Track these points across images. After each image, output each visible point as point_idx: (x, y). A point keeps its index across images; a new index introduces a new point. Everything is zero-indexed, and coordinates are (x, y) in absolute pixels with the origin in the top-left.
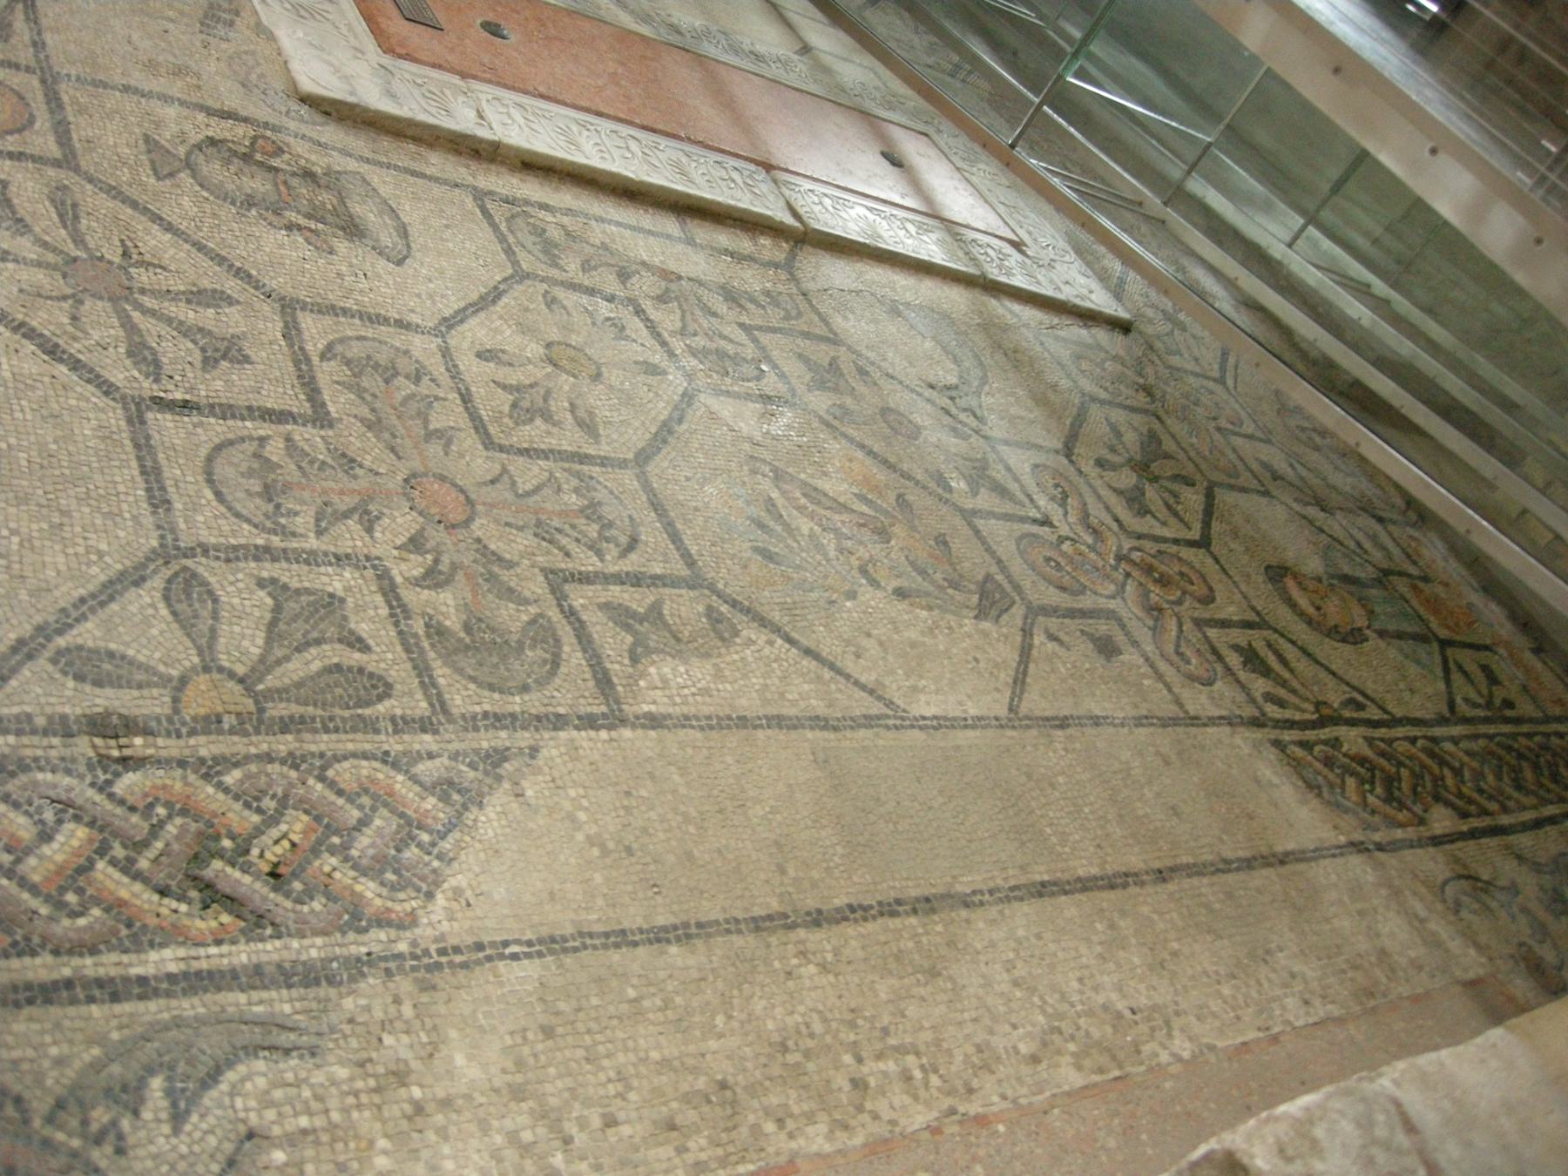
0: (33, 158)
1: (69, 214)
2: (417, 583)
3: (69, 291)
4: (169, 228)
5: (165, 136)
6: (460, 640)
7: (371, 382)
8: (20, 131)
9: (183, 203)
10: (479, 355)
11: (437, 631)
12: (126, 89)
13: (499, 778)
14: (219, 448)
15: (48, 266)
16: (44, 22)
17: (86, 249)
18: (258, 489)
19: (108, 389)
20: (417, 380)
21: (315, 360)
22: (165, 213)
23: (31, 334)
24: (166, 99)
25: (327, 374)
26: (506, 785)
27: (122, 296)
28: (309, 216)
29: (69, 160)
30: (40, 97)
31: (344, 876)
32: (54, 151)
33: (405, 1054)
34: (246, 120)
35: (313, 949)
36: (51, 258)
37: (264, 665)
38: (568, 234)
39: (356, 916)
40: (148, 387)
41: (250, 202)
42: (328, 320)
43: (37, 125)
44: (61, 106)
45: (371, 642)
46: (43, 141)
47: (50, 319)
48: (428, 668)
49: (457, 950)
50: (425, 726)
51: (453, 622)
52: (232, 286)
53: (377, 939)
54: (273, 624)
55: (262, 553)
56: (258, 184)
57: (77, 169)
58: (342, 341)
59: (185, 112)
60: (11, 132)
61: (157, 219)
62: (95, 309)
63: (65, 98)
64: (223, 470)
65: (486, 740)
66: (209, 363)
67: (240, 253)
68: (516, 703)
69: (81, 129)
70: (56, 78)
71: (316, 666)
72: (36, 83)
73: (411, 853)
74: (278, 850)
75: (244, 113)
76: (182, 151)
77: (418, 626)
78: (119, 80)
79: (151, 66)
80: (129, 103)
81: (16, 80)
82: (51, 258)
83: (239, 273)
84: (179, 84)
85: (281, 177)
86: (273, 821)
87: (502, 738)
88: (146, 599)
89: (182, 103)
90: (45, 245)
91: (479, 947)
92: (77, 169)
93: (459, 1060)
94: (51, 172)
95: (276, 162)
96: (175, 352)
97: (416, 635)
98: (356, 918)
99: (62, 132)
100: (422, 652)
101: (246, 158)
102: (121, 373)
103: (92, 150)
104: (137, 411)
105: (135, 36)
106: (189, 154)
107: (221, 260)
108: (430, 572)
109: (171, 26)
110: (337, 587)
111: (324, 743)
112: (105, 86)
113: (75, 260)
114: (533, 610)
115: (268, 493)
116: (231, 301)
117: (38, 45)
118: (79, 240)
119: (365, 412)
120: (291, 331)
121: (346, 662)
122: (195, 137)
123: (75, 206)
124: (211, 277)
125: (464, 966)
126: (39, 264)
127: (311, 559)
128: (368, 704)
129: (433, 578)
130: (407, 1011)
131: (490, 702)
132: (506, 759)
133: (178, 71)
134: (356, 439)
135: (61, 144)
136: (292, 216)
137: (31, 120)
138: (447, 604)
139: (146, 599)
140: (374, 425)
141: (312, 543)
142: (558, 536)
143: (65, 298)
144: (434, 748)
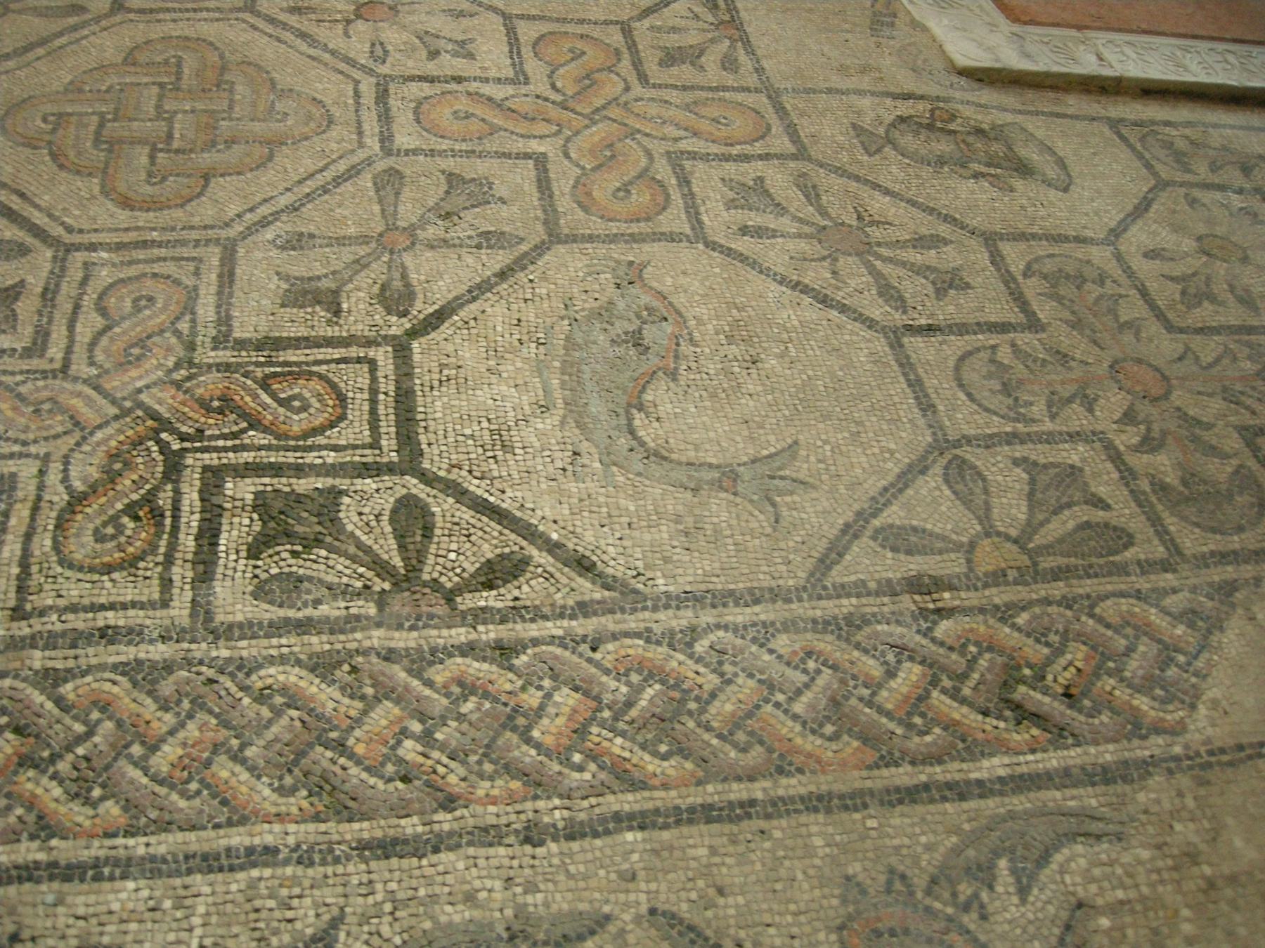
0: (777, 156)
1: (812, 194)
2: (1136, 449)
3: (826, 253)
4: (887, 192)
5: (867, 121)
6: (1181, 493)
7: (1066, 290)
8: (762, 137)
9: (892, 170)
10: (1146, 255)
11: (1162, 488)
12: (830, 91)
13: (1233, 606)
14: (962, 359)
15: (807, 236)
16: (759, 52)
17: (830, 218)
18: (998, 387)
19: (870, 324)
20: (1102, 284)
21: (1020, 279)
22: (883, 181)
23: (806, 290)
24: (860, 93)
25: (1031, 288)
26: (1240, 611)
27: (865, 250)
28: (988, 165)
29: (801, 154)
30: (771, 110)
31: (1122, 694)
32: (792, 149)
33: (1195, 839)
34: (922, 97)
35: (1108, 754)
36: (807, 229)
37: (1031, 528)
38: (1192, 143)
39: (1137, 726)
40: (899, 318)
41: (941, 161)
42: (1022, 246)
43: (774, 131)
44: (787, 114)
46: (780, 143)
47: (818, 276)
48: (1159, 519)
49: (1222, 751)
50: (1166, 567)
51: (1172, 479)
52: (944, 230)
53: (1156, 745)
54: (1031, 495)
55: (1012, 438)
56: (943, 146)
57: (809, 159)
58: (1037, 260)
59: (877, 100)
60: (756, 140)
61: (876, 186)
62: (848, 263)
63: (788, 107)
64: (969, 376)
65: (1218, 574)
66: (940, 293)
67: (943, 202)
68: (1235, 542)
69: (806, 128)
70: (778, 92)
71: (1071, 525)
72: (765, 100)
73: (1172, 672)
74: (1067, 675)
75: (920, 92)
76: (881, 131)
77: (1145, 485)
78: (823, 85)
79: (843, 69)
80: (834, 101)
81: (750, 99)
82: (807, 229)
83: (947, 219)
84: (867, 79)
85: (960, 137)
86: (1059, 652)
87: (1230, 572)
88: (931, 484)
89: (873, 94)
90: (800, 220)
91: (1240, 748)
92: (809, 159)
93: (1238, 843)
94: (792, 164)
95: (952, 127)
96: (913, 287)
97: (1144, 493)
98: (1137, 728)
99: (792, 132)
100: (1152, 506)
101: (930, 127)
102: (878, 310)
103: (816, 143)
104: (895, 336)
105: (826, 50)
106: (887, 132)
107: (932, 211)
108: (1146, 439)
109: (849, 36)
110: (1075, 459)
111: (1087, 586)
112: (814, 91)
113: (824, 228)
114: (1235, 462)
115: (1006, 389)
116: (946, 242)
117: (759, 70)
118: (824, 213)
119: (1067, 315)
120: (996, 259)
121: (1094, 520)
122: (889, 119)
123: (814, 187)
124: (928, 226)
125: (1231, 764)
126: (799, 236)
127: (1050, 439)
128: (1117, 552)
129: (1149, 444)
130: (1190, 802)
131: (1214, 543)
132: (1236, 590)
133: (864, 70)
134: (1066, 339)
135: (794, 142)
136: (976, 166)
137: (769, 128)
138: (1164, 464)
139: (931, 484)
140: (1077, 324)
141: (1048, 426)
142: (1243, 398)
143: (824, 258)
144: (1176, 583)
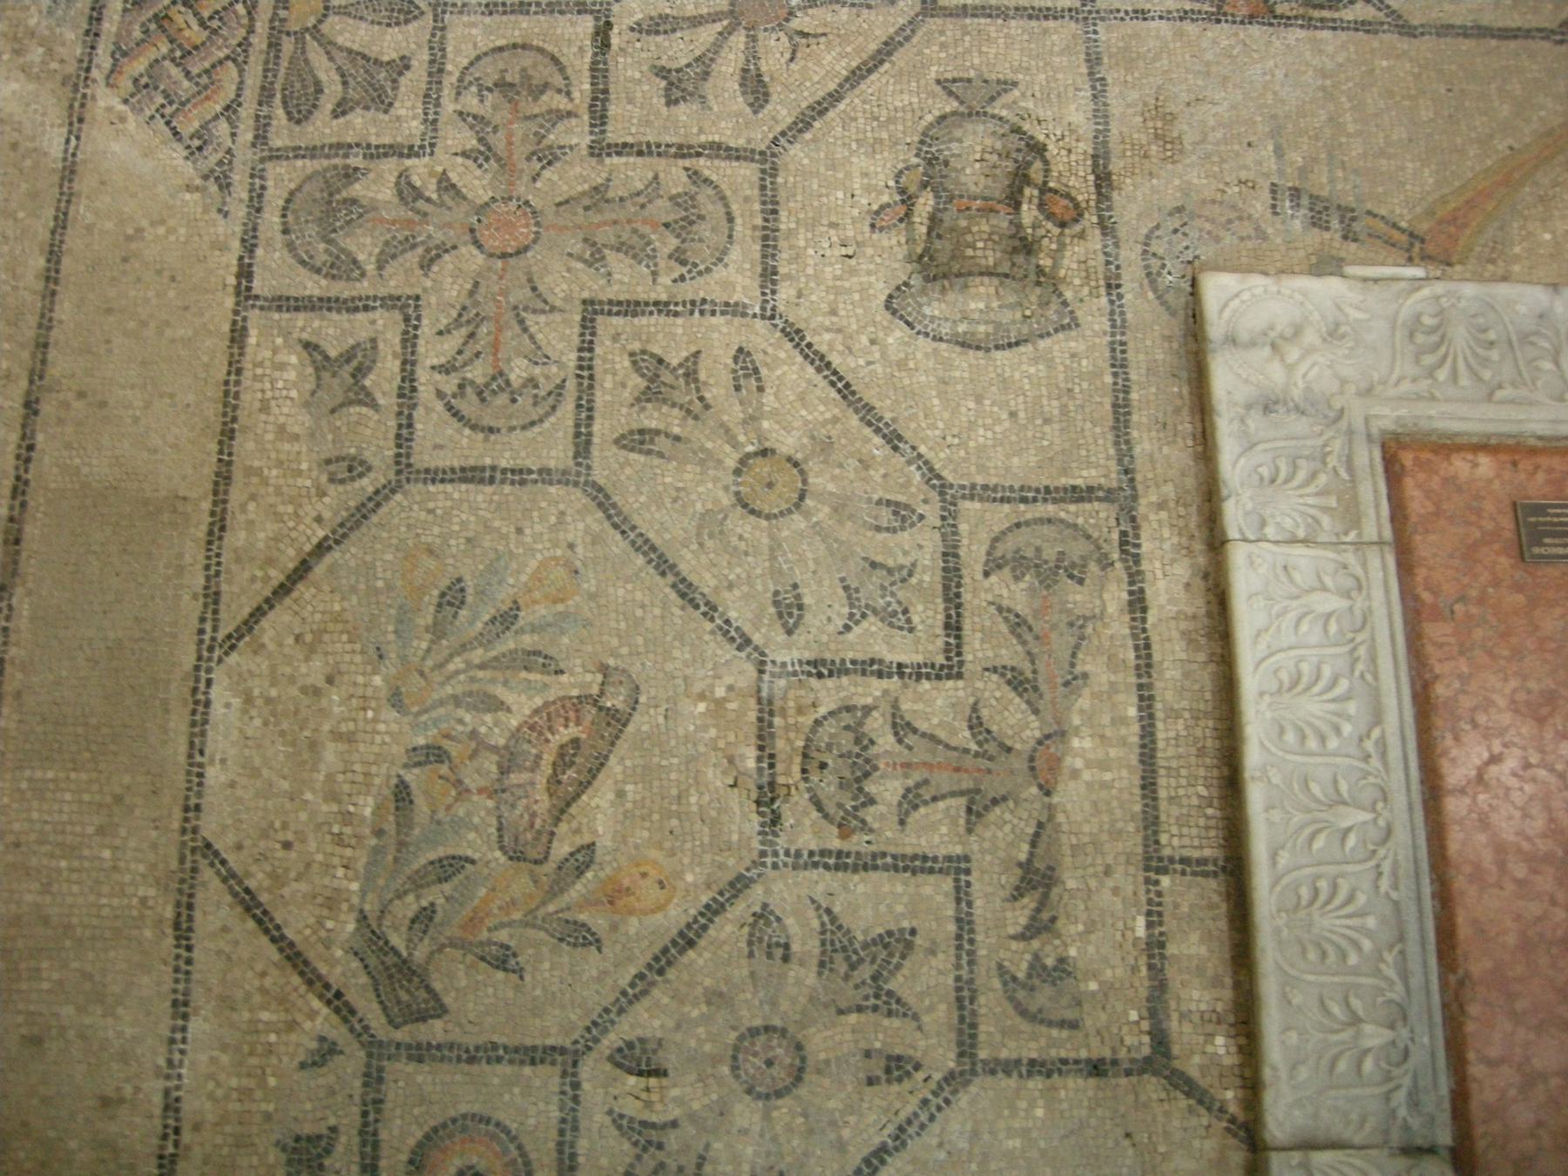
6: (339, 191)
11: (350, 175)
13: (206, 177)
18: (509, 79)
24: (1101, 115)
26: (198, 182)
31: (152, 54)
33: (29, 57)
35: (109, 26)
37: (329, 46)
39: (125, 54)
45: (342, 120)
48: (313, 157)
49: (83, 105)
50: (260, 138)
51: (357, 189)
53: (103, 59)
54: (364, 57)
55: (437, 70)
65: (239, 178)
68: (271, 219)
71: (322, 76)
73: (160, 100)
77: (356, 161)
86: (202, 24)
87: (241, 192)
91: (81, 120)
93: (15, 86)
97: (346, 156)
98: (120, 53)
100: (328, 157)
108: (418, 194)
110: (400, 110)
114: (370, 268)
121: (323, 98)
125: (71, 107)
128: (285, 103)
129: (408, 192)
130: (54, 65)
131: (275, 198)
132: (221, 187)
141: (449, 106)
142: (464, 331)
144: (239, 139)
